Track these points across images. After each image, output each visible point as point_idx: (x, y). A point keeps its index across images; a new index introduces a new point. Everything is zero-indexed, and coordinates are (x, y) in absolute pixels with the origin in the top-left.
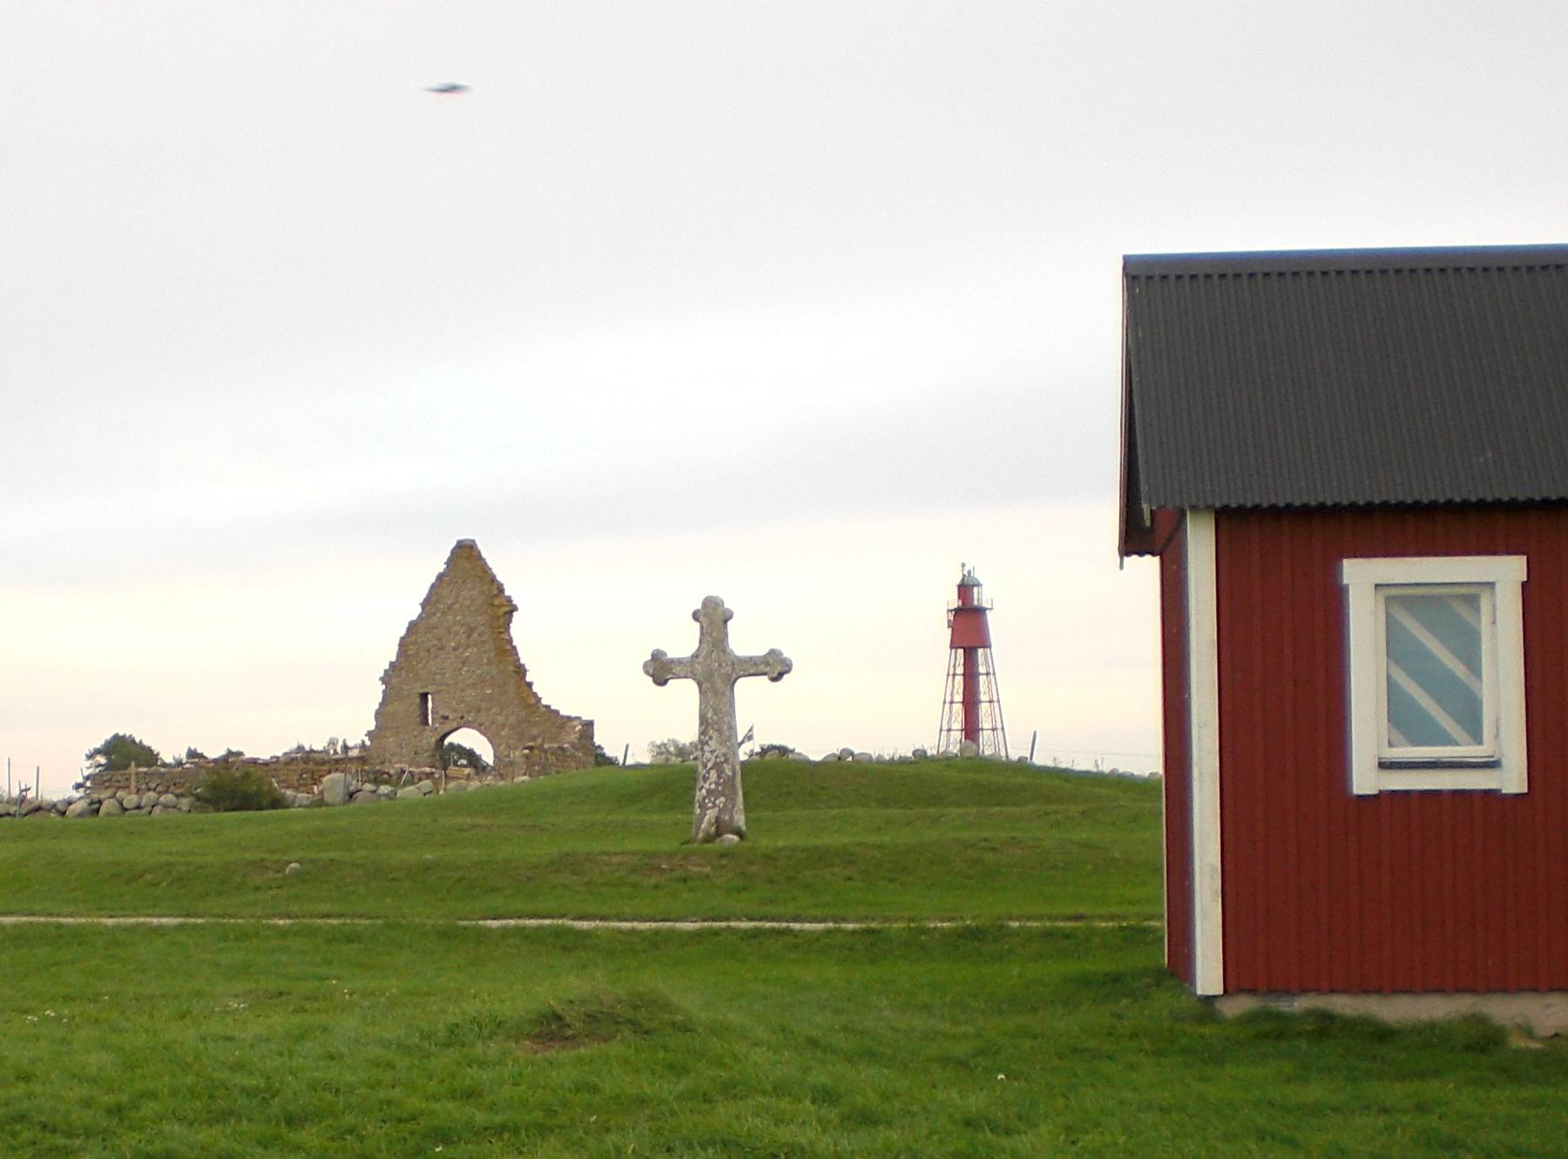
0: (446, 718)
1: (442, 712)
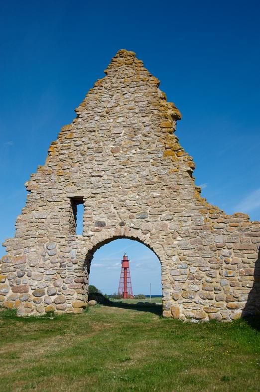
0: (101, 225)
1: (96, 218)
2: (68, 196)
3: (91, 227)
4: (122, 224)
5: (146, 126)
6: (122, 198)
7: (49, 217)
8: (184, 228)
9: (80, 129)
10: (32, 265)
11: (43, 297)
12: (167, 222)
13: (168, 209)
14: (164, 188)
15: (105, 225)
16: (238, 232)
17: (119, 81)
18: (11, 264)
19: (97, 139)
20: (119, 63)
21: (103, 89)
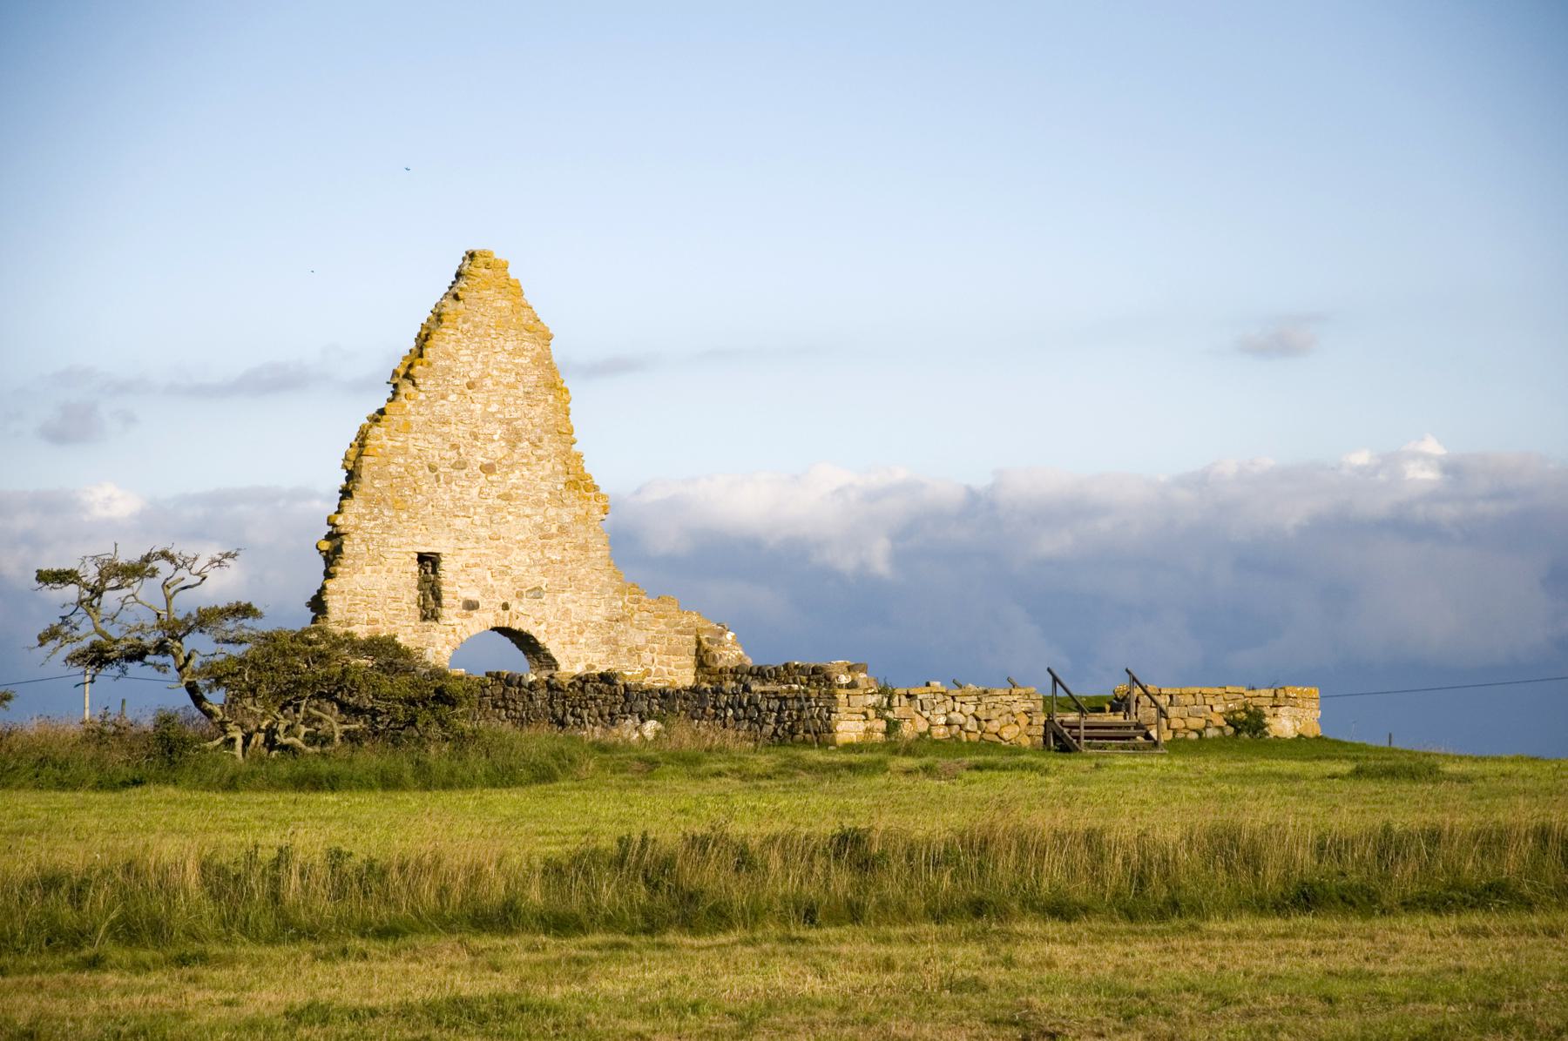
3: (456, 610)
7: (384, 587)
19: (456, 441)
21: (460, 335)
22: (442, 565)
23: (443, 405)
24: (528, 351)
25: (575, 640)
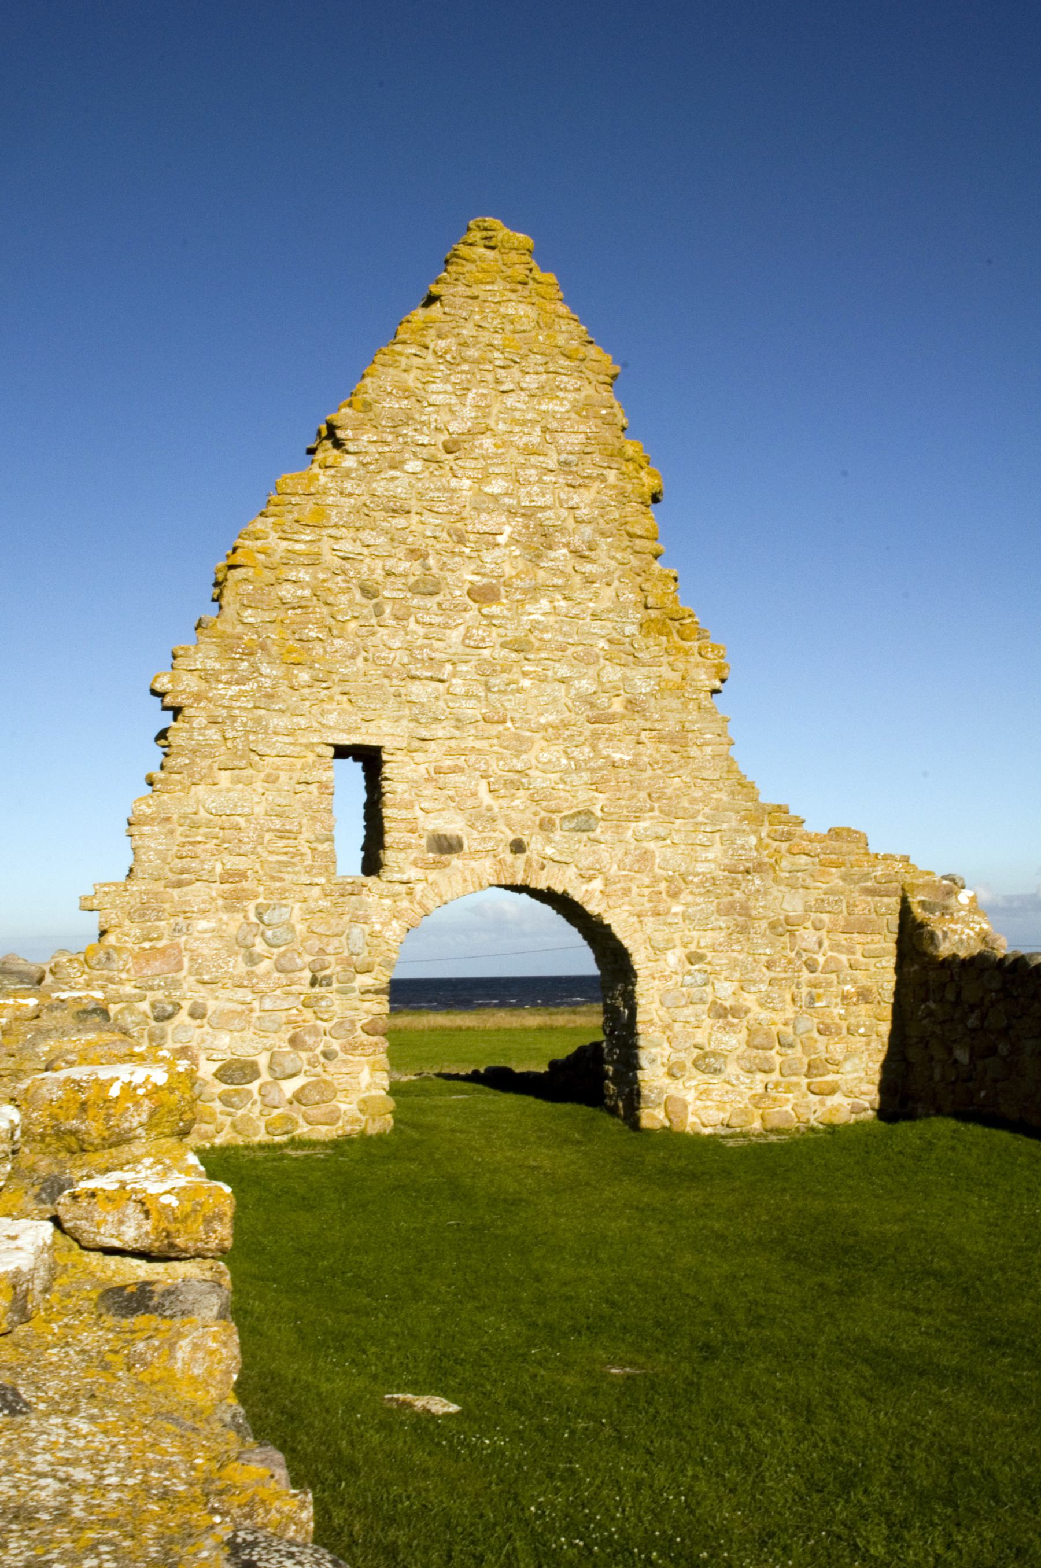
2: (330, 741)
3: (414, 854)
4: (518, 847)
5: (583, 522)
6: (515, 761)
7: (259, 810)
8: (701, 868)
9: (350, 495)
10: (206, 977)
11: (254, 1086)
12: (652, 845)
13: (656, 805)
14: (644, 736)
15: (460, 845)
16: (841, 883)
17: (485, 337)
18: (124, 976)
19: (420, 543)
20: (484, 271)
21: (430, 359)
22: (387, 771)
23: (393, 479)
24: (566, 390)
25: (661, 907)
